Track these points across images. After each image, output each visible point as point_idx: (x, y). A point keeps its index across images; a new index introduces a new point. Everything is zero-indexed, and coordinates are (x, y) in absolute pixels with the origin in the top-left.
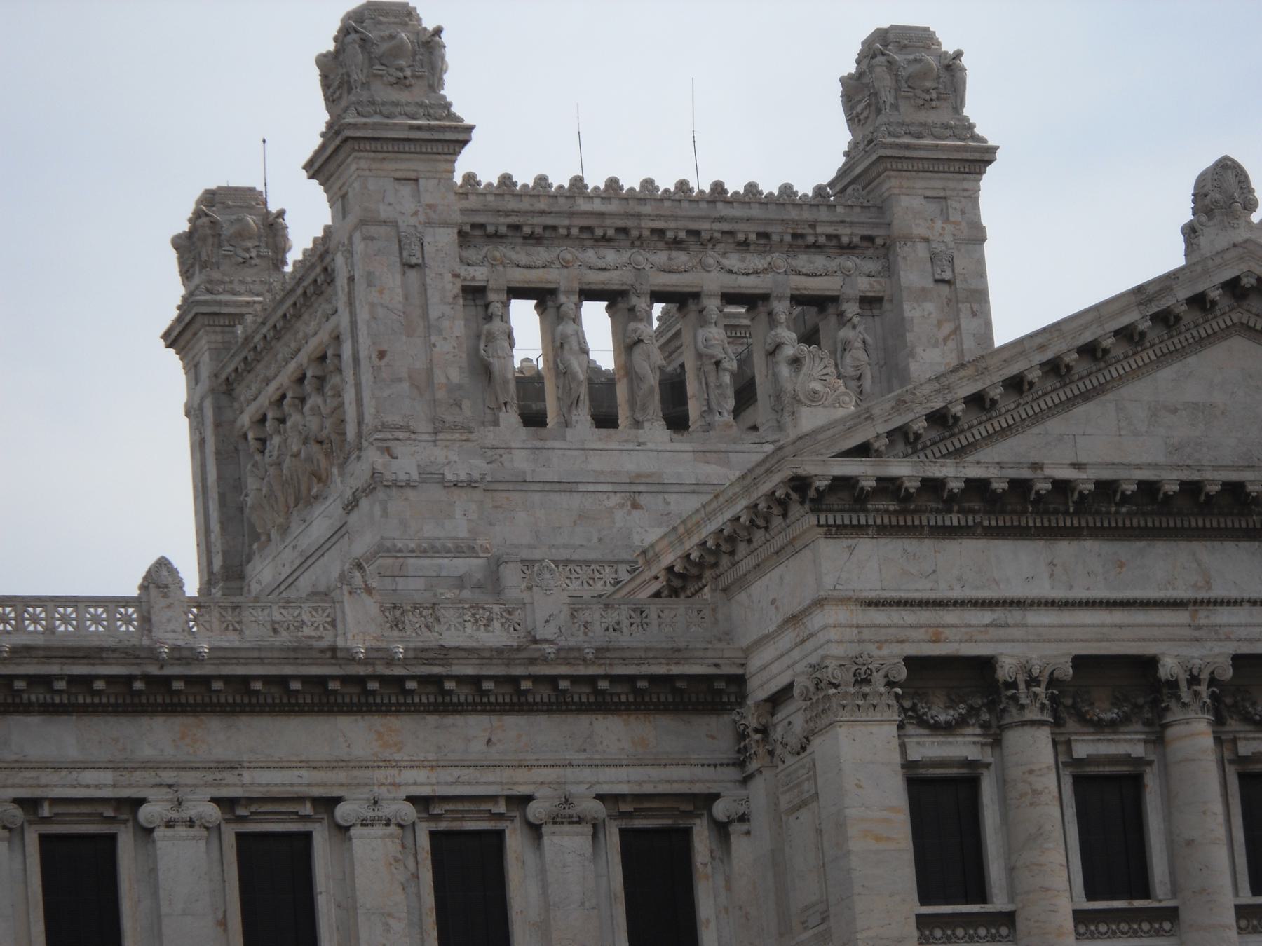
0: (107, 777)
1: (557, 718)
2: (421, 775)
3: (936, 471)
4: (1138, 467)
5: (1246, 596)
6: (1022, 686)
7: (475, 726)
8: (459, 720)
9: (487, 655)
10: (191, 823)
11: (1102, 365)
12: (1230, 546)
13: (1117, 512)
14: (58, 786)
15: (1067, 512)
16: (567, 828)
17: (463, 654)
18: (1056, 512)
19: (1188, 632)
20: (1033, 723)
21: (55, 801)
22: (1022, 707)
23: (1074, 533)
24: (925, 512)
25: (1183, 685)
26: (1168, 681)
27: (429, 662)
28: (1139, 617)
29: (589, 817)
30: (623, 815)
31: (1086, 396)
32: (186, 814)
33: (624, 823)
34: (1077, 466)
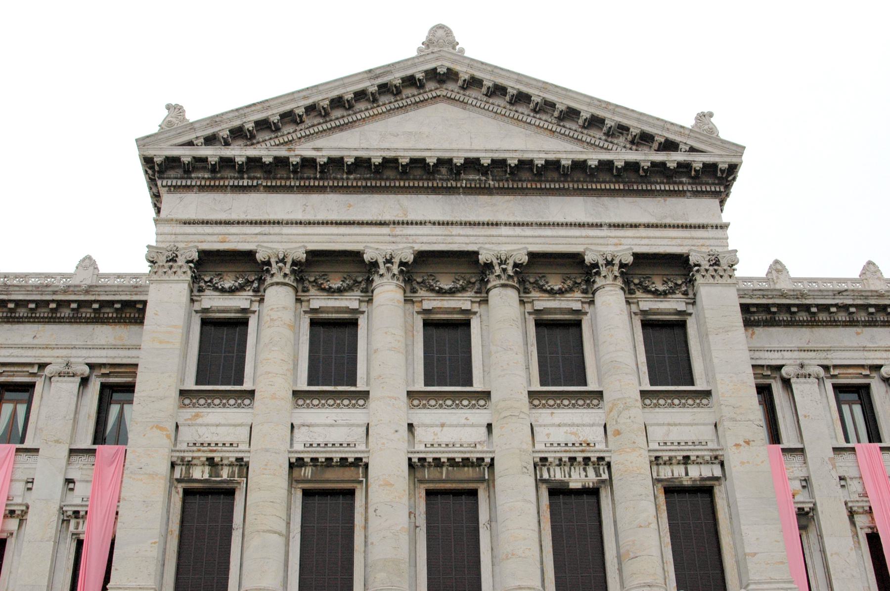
1: (75, 326)
3: (227, 152)
4: (355, 149)
5: (427, 219)
6: (274, 264)
8: (21, 326)
9: (30, 289)
11: (351, 112)
12: (423, 197)
13: (348, 179)
15: (315, 178)
16: (66, 379)
17: (17, 289)
18: (309, 178)
20: (277, 284)
22: (273, 275)
23: (321, 190)
24: (227, 178)
25: (381, 265)
26: (371, 263)
29: (79, 373)
30: (104, 375)
31: (340, 128)
33: (104, 380)
34: (314, 149)
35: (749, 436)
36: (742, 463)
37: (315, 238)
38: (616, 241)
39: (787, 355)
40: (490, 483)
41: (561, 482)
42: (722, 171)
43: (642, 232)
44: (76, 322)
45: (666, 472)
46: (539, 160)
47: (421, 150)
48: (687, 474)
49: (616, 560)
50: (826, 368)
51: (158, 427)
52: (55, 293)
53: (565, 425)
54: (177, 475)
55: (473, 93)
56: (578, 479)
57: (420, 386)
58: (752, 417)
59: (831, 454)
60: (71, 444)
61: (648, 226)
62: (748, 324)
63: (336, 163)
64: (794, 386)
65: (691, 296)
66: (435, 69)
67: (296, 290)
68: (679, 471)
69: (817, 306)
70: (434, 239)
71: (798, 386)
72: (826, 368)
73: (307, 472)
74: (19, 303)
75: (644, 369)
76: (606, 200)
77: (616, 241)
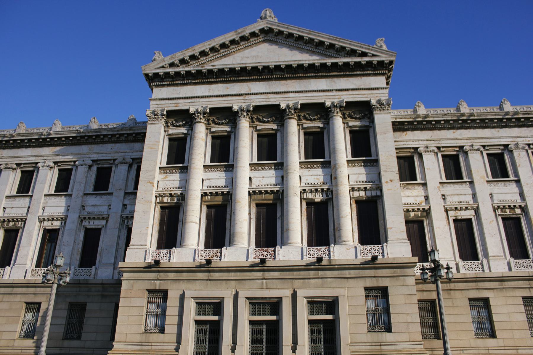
0: (34, 158)
2: (95, 155)
3: (177, 70)
4: (229, 65)
5: (259, 92)
7: (109, 146)
8: (106, 145)
10: (47, 166)
12: (258, 83)
14: (24, 161)
15: (214, 78)
18: (211, 78)
19: (243, 101)
21: (24, 164)
23: (216, 83)
27: (97, 132)
28: (230, 98)
31: (225, 56)
32: (45, 165)
35: (392, 178)
36: (389, 190)
37: (213, 103)
38: (339, 97)
39: (421, 142)
40: (282, 201)
41: (312, 199)
42: (386, 64)
43: (350, 92)
44: (127, 142)
45: (356, 194)
46: (306, 63)
47: (256, 63)
48: (366, 195)
49: (333, 231)
50: (439, 148)
51: (149, 182)
52: (118, 131)
53: (314, 175)
54: (158, 201)
55: (280, 37)
56: (318, 198)
57: (255, 161)
58: (394, 170)
59: (439, 185)
60: (125, 190)
61: (353, 90)
62: (395, 130)
63: (221, 71)
64: (424, 156)
65: (371, 119)
66: (264, 28)
67: (206, 125)
68: (362, 193)
69: (435, 121)
70: (261, 100)
71: (425, 157)
72: (439, 148)
73: (208, 198)
74: (105, 136)
75: (349, 151)
76: (335, 80)
77: (339, 97)
